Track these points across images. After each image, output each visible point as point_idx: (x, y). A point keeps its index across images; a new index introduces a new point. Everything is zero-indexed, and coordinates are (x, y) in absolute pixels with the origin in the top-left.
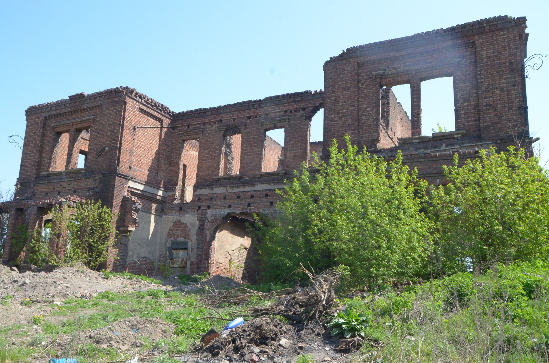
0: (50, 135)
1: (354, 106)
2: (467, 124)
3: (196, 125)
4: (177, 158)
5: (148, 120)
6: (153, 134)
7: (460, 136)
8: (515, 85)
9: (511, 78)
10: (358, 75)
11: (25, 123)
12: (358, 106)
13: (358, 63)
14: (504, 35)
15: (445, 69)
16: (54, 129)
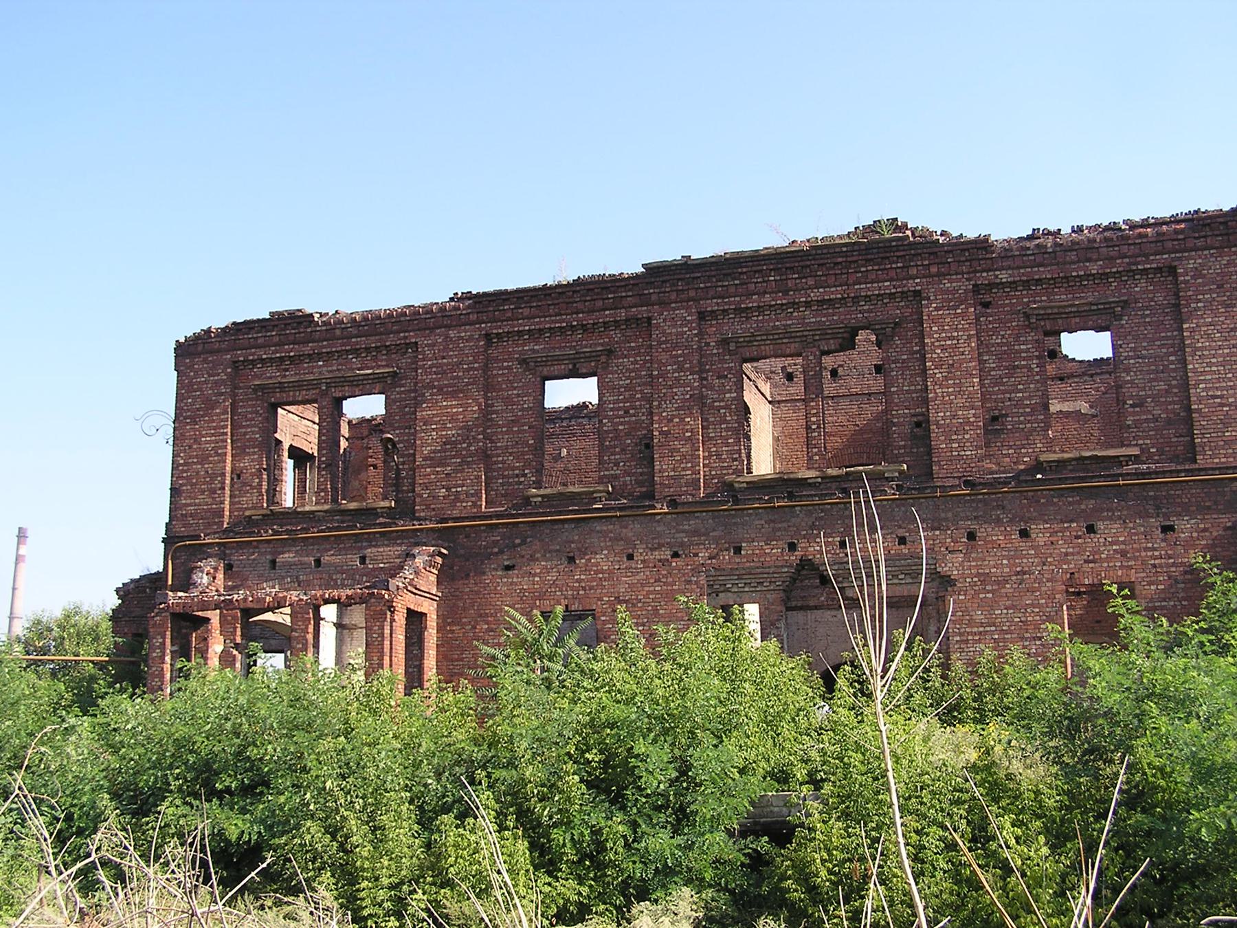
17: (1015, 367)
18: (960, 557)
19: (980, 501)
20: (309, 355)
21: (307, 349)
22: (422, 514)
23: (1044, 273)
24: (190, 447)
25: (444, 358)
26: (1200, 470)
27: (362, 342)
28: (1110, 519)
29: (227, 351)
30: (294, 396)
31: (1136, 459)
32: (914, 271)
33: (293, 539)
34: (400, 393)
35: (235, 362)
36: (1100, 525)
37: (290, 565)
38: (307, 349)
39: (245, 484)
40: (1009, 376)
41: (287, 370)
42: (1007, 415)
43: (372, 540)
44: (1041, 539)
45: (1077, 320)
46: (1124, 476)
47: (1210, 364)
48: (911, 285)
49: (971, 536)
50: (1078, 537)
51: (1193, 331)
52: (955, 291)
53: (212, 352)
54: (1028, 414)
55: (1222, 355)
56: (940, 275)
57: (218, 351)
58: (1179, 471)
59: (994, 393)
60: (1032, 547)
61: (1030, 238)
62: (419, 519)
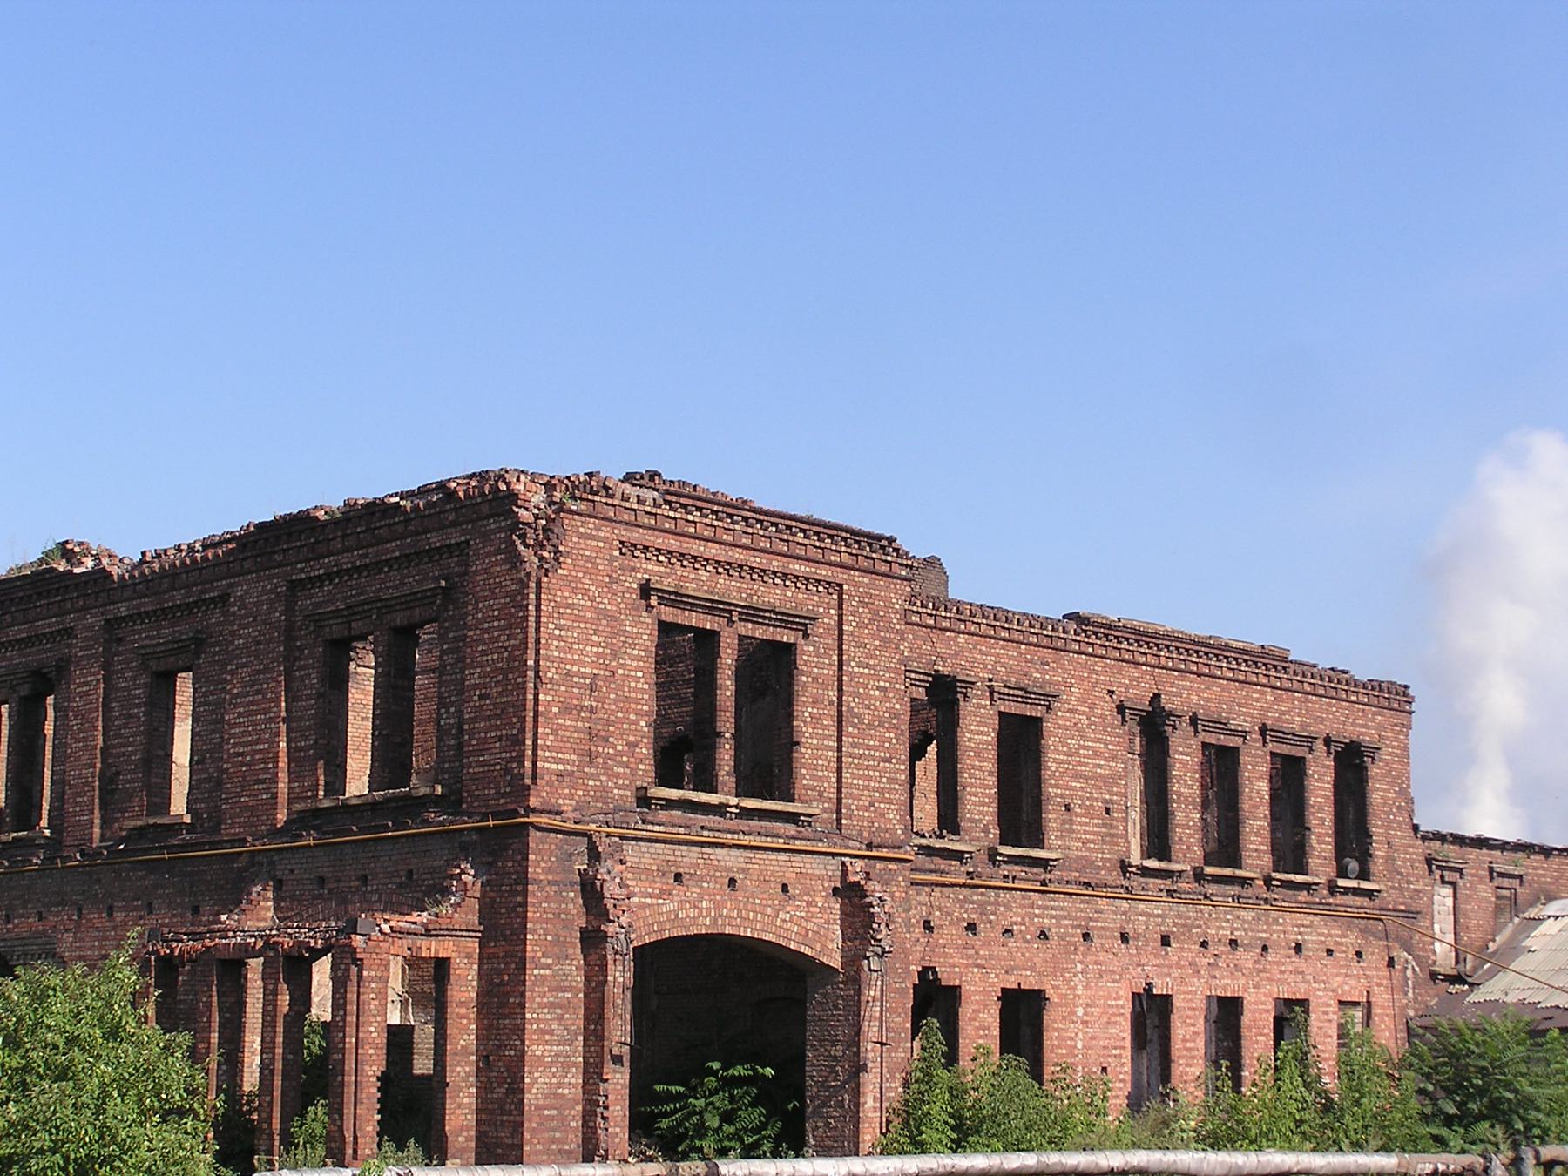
17: (131, 716)
18: (69, 937)
19: (89, 873)
23: (148, 604)
26: (219, 842)
28: (161, 897)
31: (191, 828)
32: (69, 605)
36: (155, 904)
40: (125, 726)
42: (118, 773)
44: (119, 916)
45: (172, 659)
46: (171, 849)
47: (240, 715)
48: (69, 620)
49: (80, 910)
50: (141, 918)
51: (233, 673)
52: (90, 628)
54: (130, 772)
55: (248, 704)
56: (84, 609)
58: (204, 844)
59: (114, 747)
60: (114, 928)
61: (142, 562)
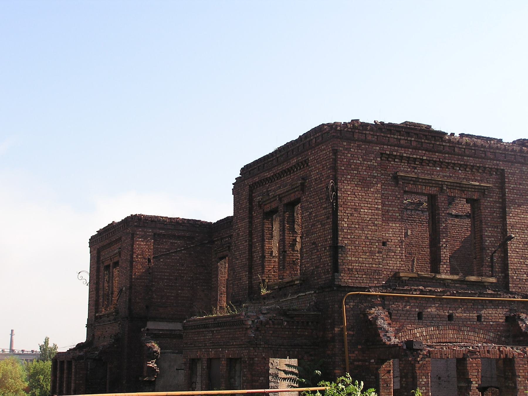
0: (102, 269)
1: (246, 242)
2: (307, 265)
3: (225, 238)
4: (215, 281)
5: (171, 243)
6: (181, 258)
7: (298, 282)
8: (328, 218)
9: (325, 208)
10: (251, 200)
11: (89, 255)
12: (251, 240)
13: (250, 186)
14: (324, 150)
15: (297, 193)
16: (103, 262)
20: (435, 161)
21: (436, 156)
22: (514, 290)
24: (352, 215)
25: (520, 184)
27: (471, 161)
29: (377, 143)
30: (421, 189)
33: (438, 298)
34: (490, 202)
35: (382, 154)
37: (432, 317)
38: (436, 156)
39: (389, 250)
41: (415, 168)
43: (484, 304)
53: (365, 141)
57: (370, 142)
62: (512, 293)
